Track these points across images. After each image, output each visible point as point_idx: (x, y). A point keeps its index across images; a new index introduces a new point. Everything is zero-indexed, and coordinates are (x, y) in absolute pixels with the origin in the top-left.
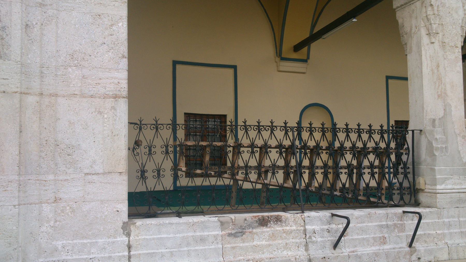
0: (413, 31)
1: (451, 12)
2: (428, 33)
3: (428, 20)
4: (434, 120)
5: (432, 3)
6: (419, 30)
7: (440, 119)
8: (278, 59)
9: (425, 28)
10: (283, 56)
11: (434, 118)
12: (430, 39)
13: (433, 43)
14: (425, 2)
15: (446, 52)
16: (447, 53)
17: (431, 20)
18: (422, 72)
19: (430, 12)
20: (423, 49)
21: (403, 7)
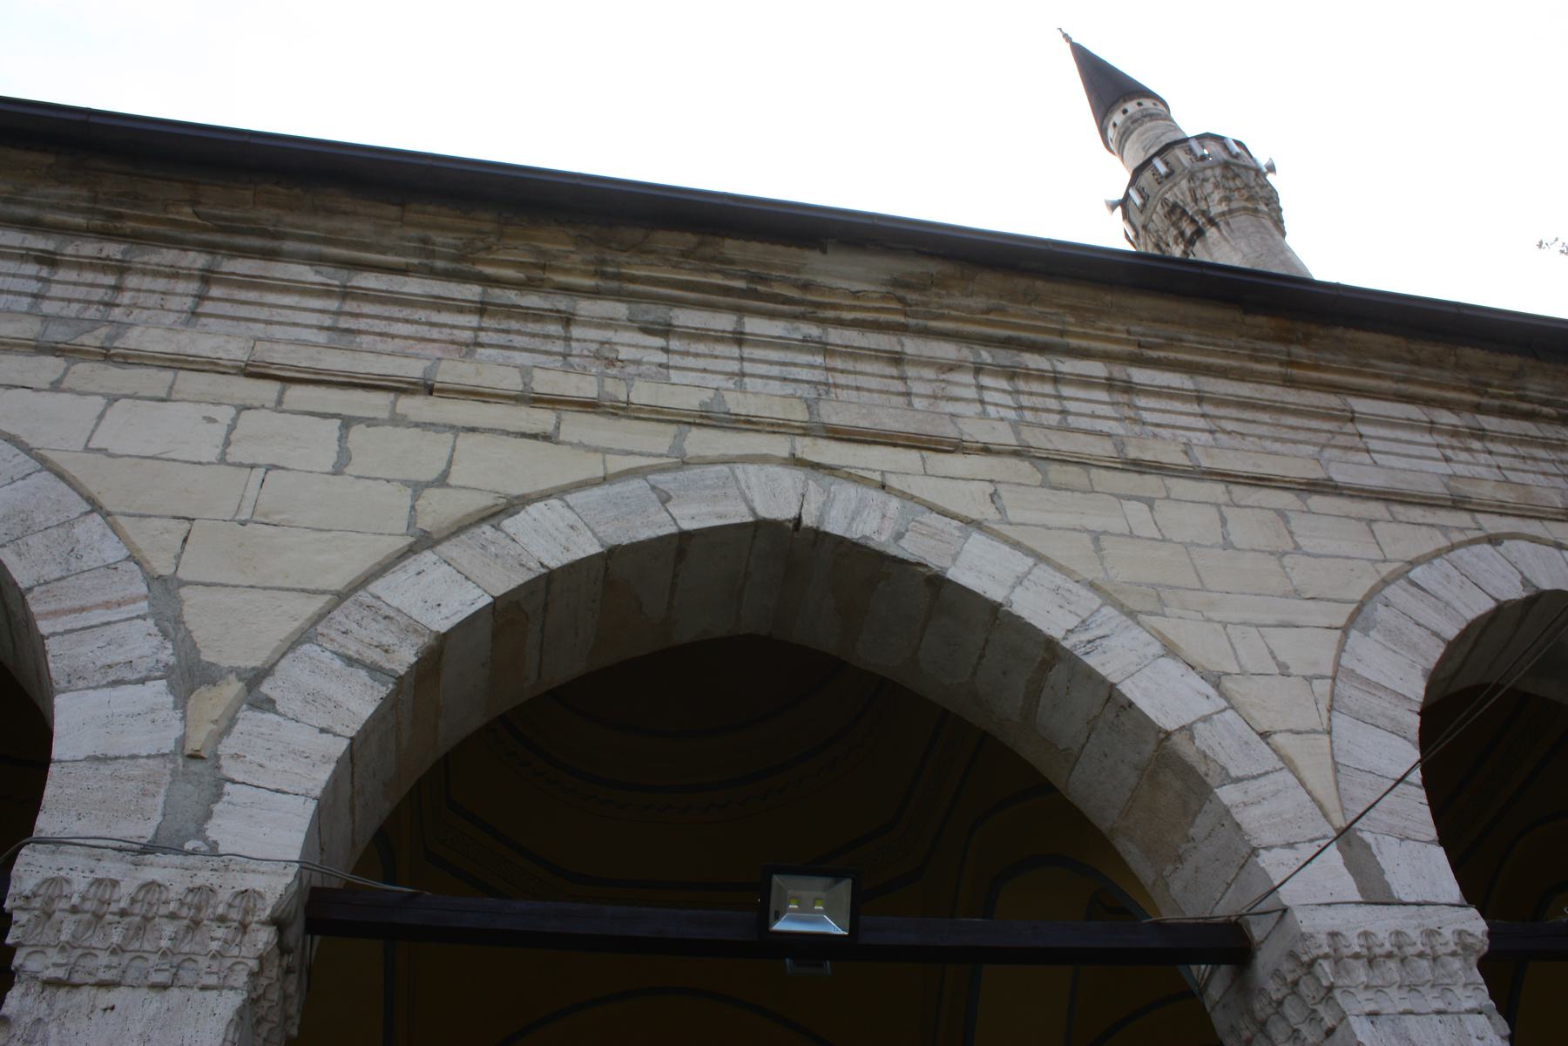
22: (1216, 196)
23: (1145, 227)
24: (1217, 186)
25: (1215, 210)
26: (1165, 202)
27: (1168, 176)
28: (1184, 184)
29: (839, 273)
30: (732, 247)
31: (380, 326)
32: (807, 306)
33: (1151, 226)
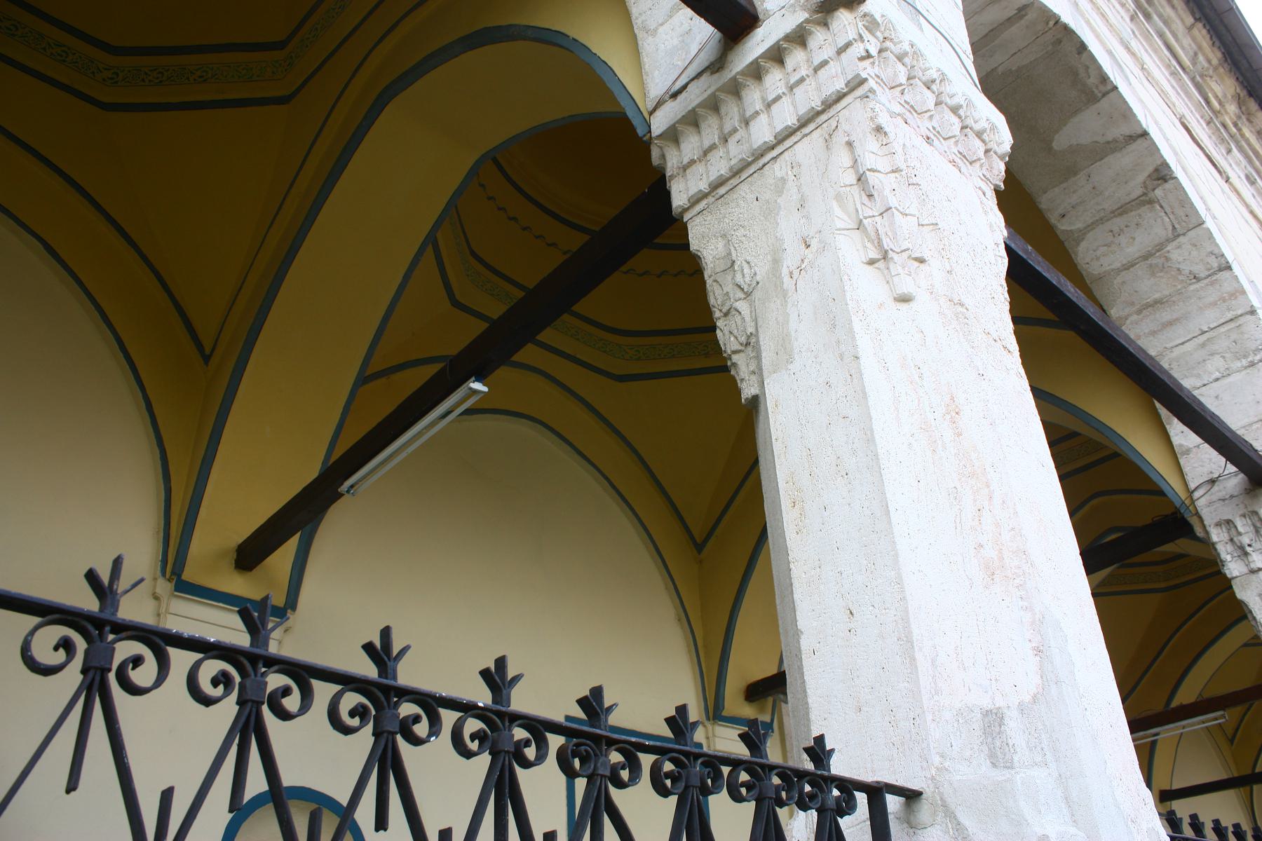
2: (874, 254)
4: (993, 720)
7: (1022, 708)
8: (164, 587)
9: (857, 235)
10: (184, 577)
11: (986, 703)
13: (905, 299)
14: (844, 126)
17: (887, 192)
18: (871, 440)
20: (857, 326)
21: (722, 191)
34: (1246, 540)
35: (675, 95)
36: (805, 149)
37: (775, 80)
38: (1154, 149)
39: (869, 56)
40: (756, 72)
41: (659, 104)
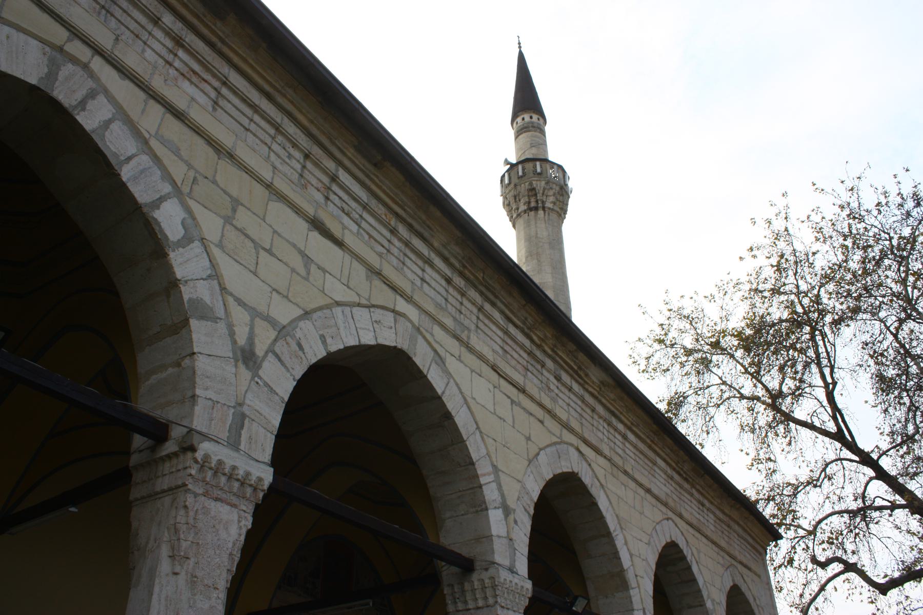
0: (150, 546)
1: (217, 527)
3: (176, 531)
5: (187, 503)
6: (159, 546)
12: (173, 565)
13: (176, 574)
15: (195, 595)
16: (196, 597)
19: (181, 519)
20: (157, 581)
22: (552, 199)
23: (515, 185)
24: (554, 195)
25: (549, 205)
26: (531, 184)
27: (540, 174)
28: (543, 183)
29: (596, 375)
30: (581, 356)
31: (515, 355)
32: (578, 374)
33: (518, 187)
34: (457, 596)
35: (141, 451)
36: (167, 500)
37: (167, 465)
38: (443, 405)
39: (191, 475)
40: (163, 459)
41: (135, 452)
